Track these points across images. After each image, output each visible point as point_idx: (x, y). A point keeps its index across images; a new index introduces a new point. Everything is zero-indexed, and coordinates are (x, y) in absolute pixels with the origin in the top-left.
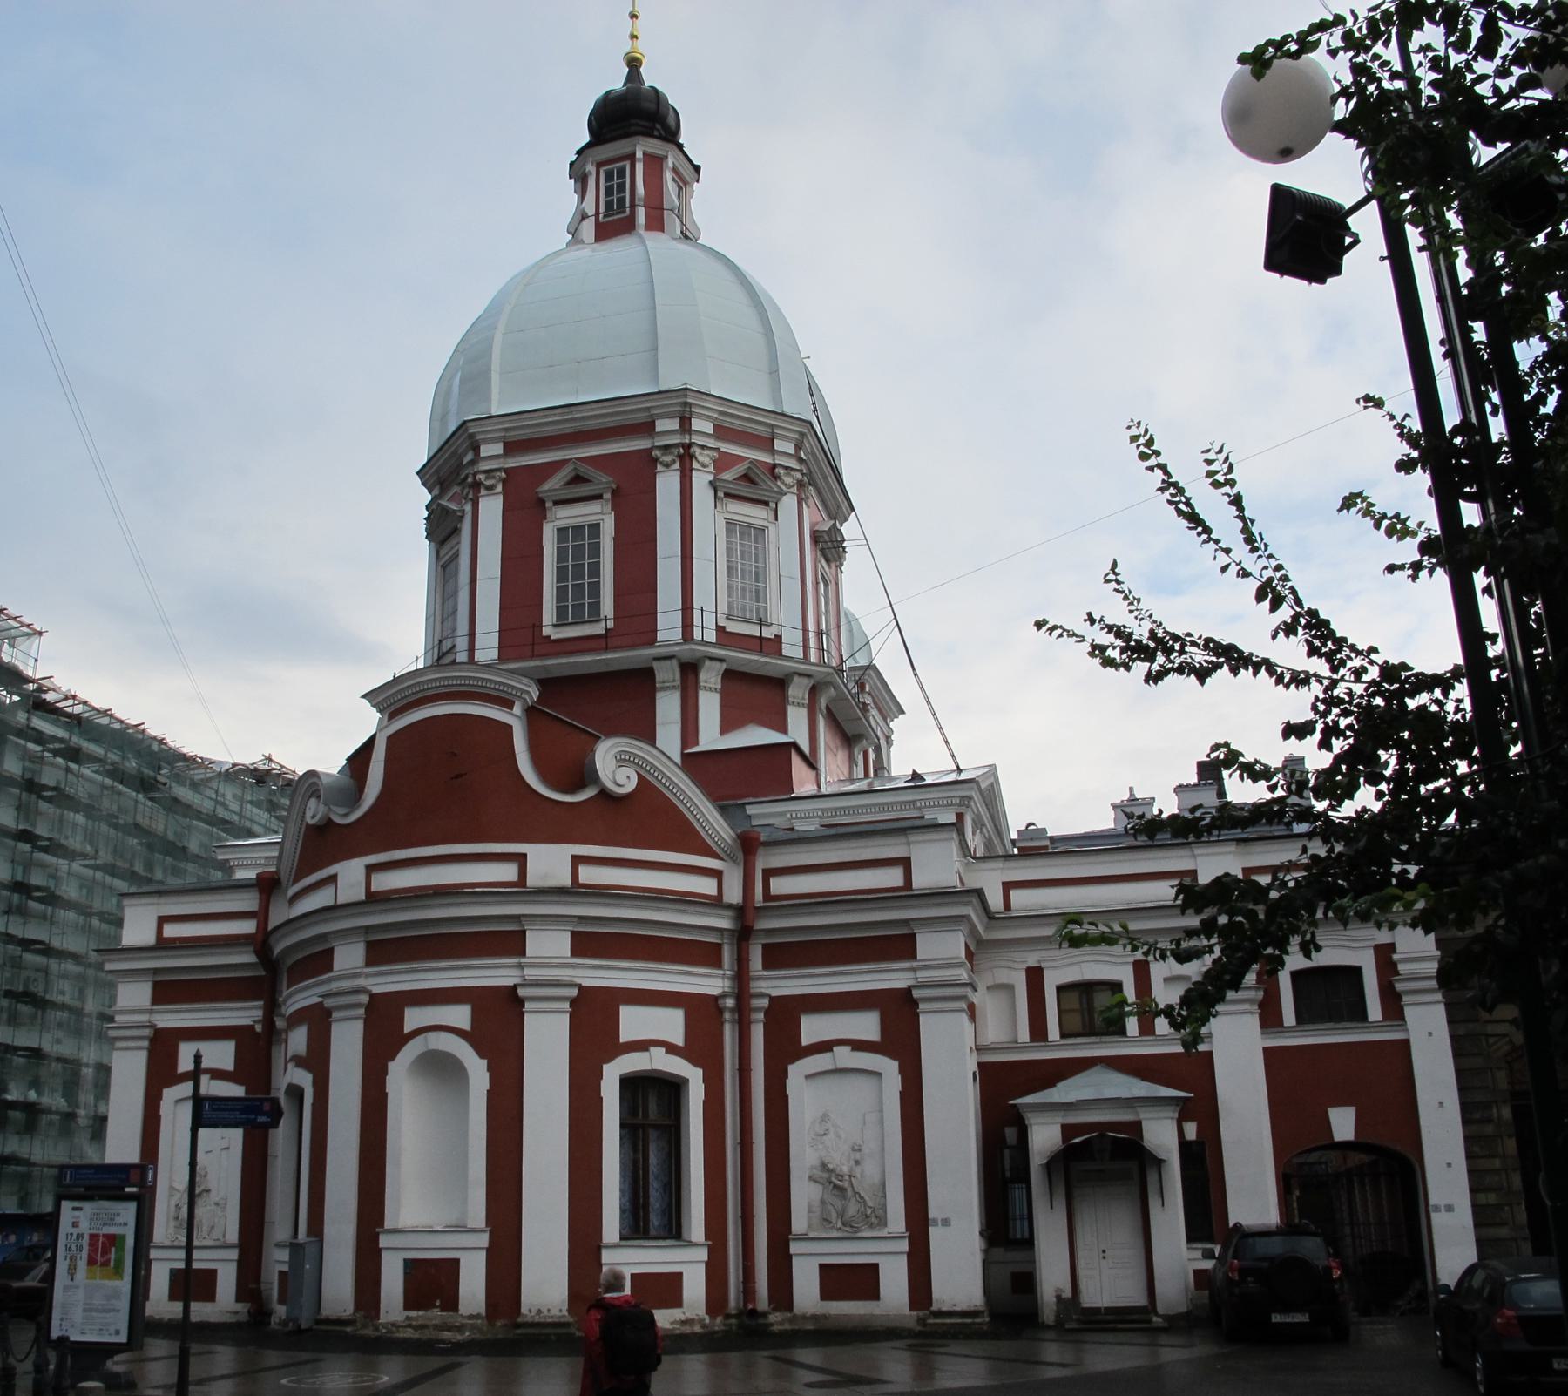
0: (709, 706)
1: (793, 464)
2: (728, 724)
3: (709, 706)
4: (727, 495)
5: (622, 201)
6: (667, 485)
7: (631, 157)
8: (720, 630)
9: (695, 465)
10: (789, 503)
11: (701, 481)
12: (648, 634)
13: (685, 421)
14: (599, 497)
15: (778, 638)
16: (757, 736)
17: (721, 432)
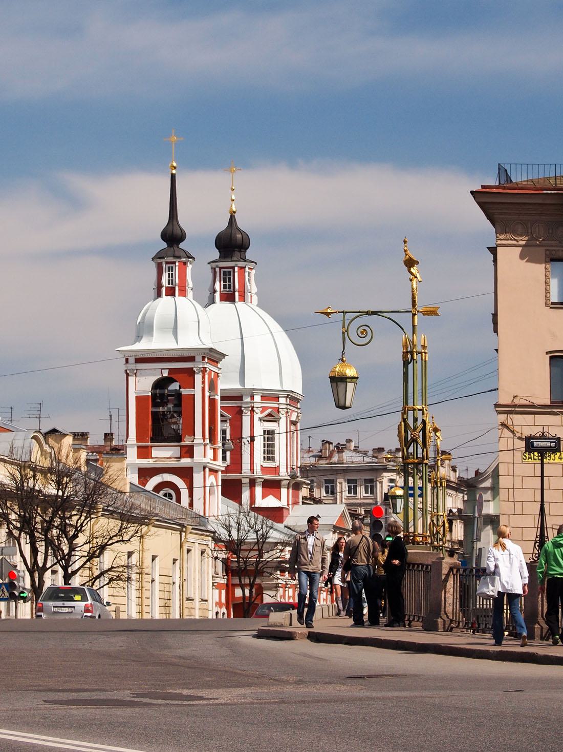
0: (259, 490)
1: (285, 406)
2: (264, 496)
3: (259, 490)
4: (264, 421)
5: (229, 285)
6: (246, 420)
7: (233, 268)
8: (261, 466)
9: (255, 413)
10: (283, 421)
11: (256, 418)
12: (240, 470)
13: (252, 397)
14: (226, 421)
15: (279, 466)
16: (271, 502)
17: (265, 398)
